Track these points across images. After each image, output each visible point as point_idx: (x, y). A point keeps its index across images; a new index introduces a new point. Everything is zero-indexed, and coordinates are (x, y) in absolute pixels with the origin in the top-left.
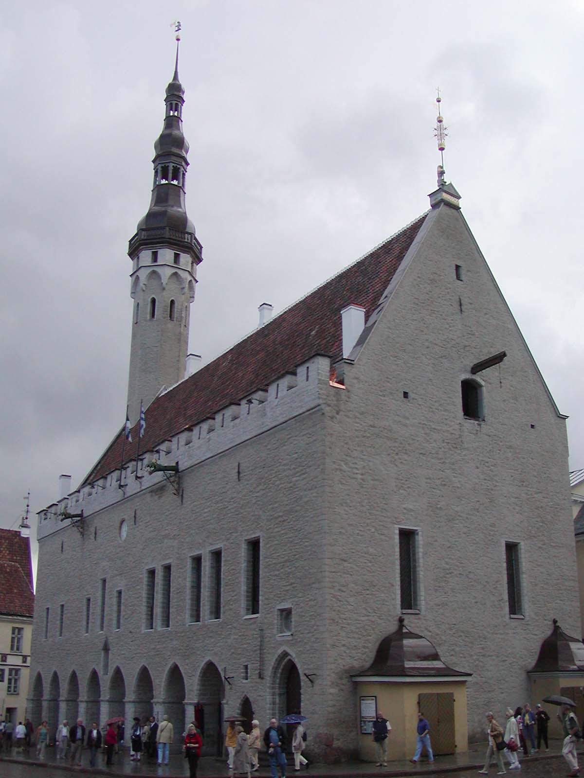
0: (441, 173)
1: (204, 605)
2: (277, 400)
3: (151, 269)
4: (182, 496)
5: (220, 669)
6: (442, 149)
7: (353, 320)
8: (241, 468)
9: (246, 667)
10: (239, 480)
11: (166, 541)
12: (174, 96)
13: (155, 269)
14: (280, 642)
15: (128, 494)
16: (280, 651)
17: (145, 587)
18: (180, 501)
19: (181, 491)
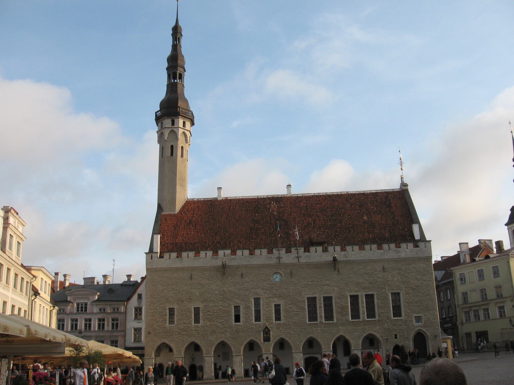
0: (402, 178)
1: (364, 314)
2: (408, 250)
3: (183, 130)
4: (338, 271)
5: (378, 336)
6: (402, 170)
7: (415, 228)
8: (385, 267)
9: (396, 336)
10: (384, 271)
11: (325, 287)
12: (176, 32)
13: (186, 132)
14: (417, 326)
15: (283, 262)
16: (417, 329)
17: (307, 304)
18: (337, 273)
19: (337, 269)
